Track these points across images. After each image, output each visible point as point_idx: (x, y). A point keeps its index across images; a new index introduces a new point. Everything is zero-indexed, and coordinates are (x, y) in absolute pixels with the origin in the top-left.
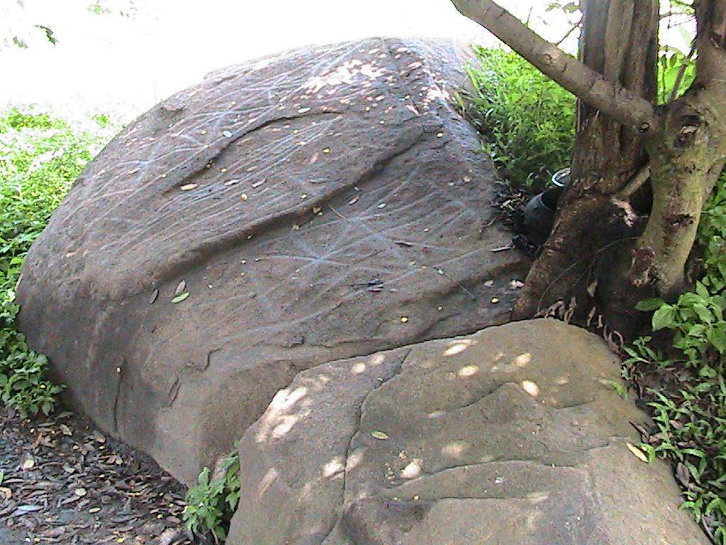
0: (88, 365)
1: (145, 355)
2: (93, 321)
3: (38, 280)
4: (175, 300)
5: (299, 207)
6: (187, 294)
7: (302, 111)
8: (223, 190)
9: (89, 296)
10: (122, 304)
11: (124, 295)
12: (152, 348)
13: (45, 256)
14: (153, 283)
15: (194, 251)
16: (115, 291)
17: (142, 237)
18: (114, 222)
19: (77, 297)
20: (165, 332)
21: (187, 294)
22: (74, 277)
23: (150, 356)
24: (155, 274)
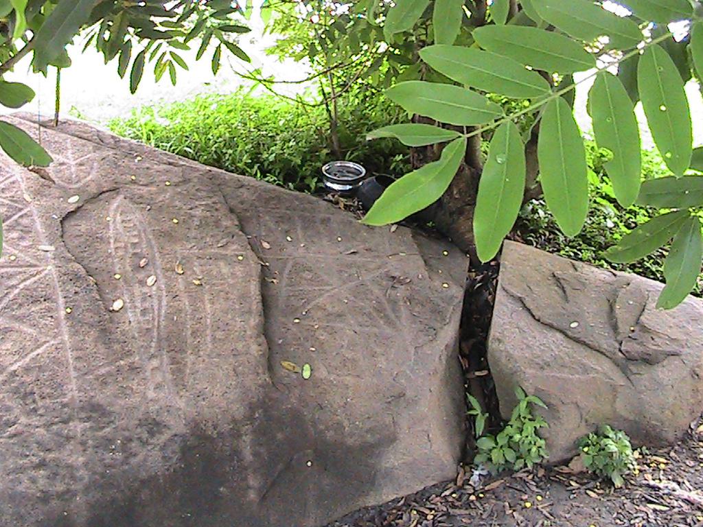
0: (252, 495)
1: (340, 424)
2: (236, 453)
3: (78, 487)
4: (306, 374)
5: (255, 269)
6: (307, 367)
7: (74, 199)
8: (159, 289)
9: (209, 439)
10: (257, 415)
11: (252, 408)
12: (341, 417)
13: (42, 464)
14: (267, 379)
15: (258, 336)
16: (239, 410)
17: (174, 361)
18: (110, 374)
19: (186, 451)
20: (335, 399)
21: (307, 367)
22: (164, 438)
23: (346, 423)
24: (260, 371)
